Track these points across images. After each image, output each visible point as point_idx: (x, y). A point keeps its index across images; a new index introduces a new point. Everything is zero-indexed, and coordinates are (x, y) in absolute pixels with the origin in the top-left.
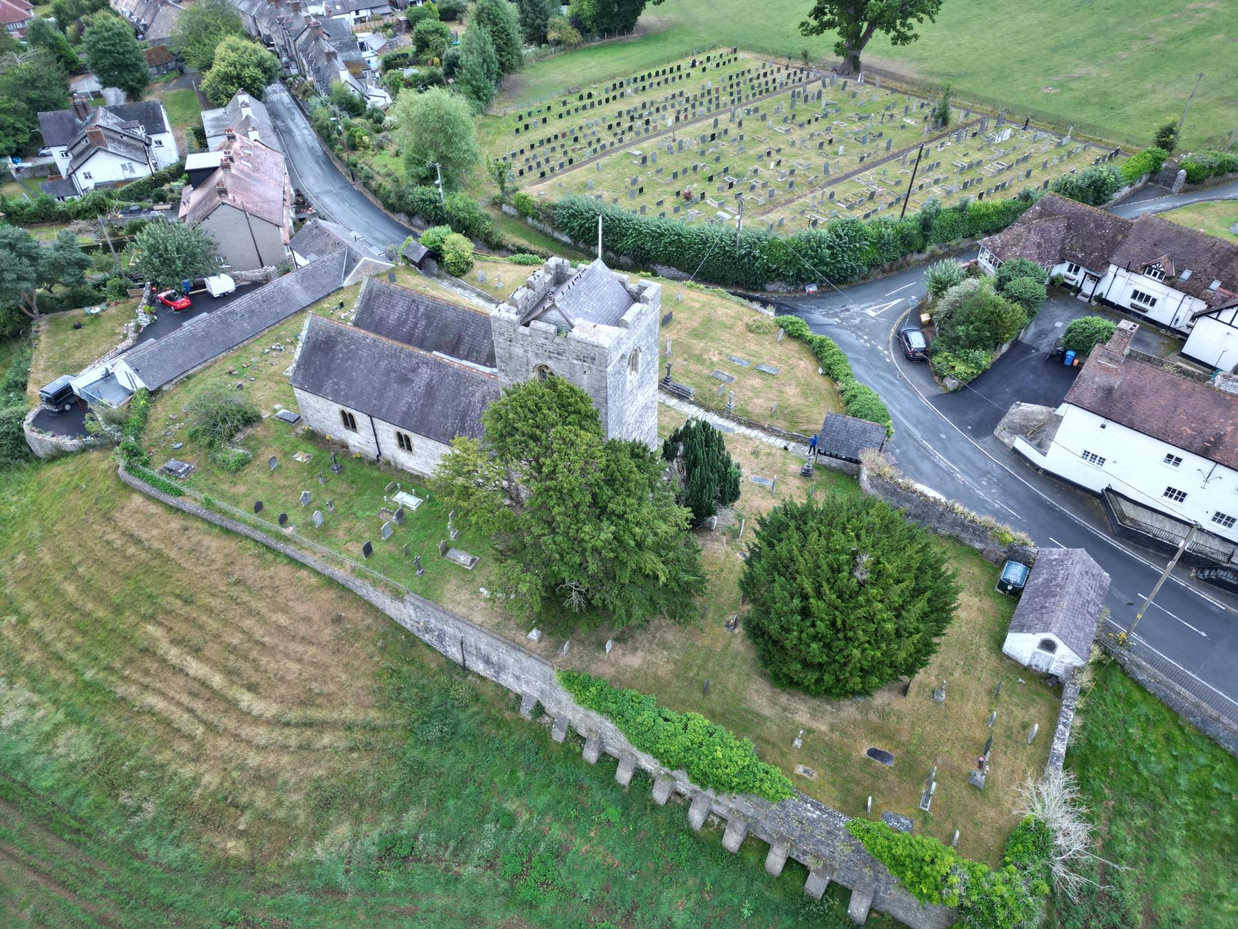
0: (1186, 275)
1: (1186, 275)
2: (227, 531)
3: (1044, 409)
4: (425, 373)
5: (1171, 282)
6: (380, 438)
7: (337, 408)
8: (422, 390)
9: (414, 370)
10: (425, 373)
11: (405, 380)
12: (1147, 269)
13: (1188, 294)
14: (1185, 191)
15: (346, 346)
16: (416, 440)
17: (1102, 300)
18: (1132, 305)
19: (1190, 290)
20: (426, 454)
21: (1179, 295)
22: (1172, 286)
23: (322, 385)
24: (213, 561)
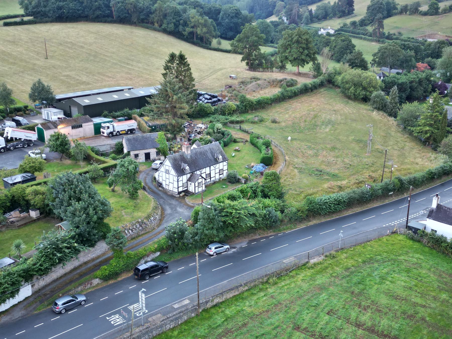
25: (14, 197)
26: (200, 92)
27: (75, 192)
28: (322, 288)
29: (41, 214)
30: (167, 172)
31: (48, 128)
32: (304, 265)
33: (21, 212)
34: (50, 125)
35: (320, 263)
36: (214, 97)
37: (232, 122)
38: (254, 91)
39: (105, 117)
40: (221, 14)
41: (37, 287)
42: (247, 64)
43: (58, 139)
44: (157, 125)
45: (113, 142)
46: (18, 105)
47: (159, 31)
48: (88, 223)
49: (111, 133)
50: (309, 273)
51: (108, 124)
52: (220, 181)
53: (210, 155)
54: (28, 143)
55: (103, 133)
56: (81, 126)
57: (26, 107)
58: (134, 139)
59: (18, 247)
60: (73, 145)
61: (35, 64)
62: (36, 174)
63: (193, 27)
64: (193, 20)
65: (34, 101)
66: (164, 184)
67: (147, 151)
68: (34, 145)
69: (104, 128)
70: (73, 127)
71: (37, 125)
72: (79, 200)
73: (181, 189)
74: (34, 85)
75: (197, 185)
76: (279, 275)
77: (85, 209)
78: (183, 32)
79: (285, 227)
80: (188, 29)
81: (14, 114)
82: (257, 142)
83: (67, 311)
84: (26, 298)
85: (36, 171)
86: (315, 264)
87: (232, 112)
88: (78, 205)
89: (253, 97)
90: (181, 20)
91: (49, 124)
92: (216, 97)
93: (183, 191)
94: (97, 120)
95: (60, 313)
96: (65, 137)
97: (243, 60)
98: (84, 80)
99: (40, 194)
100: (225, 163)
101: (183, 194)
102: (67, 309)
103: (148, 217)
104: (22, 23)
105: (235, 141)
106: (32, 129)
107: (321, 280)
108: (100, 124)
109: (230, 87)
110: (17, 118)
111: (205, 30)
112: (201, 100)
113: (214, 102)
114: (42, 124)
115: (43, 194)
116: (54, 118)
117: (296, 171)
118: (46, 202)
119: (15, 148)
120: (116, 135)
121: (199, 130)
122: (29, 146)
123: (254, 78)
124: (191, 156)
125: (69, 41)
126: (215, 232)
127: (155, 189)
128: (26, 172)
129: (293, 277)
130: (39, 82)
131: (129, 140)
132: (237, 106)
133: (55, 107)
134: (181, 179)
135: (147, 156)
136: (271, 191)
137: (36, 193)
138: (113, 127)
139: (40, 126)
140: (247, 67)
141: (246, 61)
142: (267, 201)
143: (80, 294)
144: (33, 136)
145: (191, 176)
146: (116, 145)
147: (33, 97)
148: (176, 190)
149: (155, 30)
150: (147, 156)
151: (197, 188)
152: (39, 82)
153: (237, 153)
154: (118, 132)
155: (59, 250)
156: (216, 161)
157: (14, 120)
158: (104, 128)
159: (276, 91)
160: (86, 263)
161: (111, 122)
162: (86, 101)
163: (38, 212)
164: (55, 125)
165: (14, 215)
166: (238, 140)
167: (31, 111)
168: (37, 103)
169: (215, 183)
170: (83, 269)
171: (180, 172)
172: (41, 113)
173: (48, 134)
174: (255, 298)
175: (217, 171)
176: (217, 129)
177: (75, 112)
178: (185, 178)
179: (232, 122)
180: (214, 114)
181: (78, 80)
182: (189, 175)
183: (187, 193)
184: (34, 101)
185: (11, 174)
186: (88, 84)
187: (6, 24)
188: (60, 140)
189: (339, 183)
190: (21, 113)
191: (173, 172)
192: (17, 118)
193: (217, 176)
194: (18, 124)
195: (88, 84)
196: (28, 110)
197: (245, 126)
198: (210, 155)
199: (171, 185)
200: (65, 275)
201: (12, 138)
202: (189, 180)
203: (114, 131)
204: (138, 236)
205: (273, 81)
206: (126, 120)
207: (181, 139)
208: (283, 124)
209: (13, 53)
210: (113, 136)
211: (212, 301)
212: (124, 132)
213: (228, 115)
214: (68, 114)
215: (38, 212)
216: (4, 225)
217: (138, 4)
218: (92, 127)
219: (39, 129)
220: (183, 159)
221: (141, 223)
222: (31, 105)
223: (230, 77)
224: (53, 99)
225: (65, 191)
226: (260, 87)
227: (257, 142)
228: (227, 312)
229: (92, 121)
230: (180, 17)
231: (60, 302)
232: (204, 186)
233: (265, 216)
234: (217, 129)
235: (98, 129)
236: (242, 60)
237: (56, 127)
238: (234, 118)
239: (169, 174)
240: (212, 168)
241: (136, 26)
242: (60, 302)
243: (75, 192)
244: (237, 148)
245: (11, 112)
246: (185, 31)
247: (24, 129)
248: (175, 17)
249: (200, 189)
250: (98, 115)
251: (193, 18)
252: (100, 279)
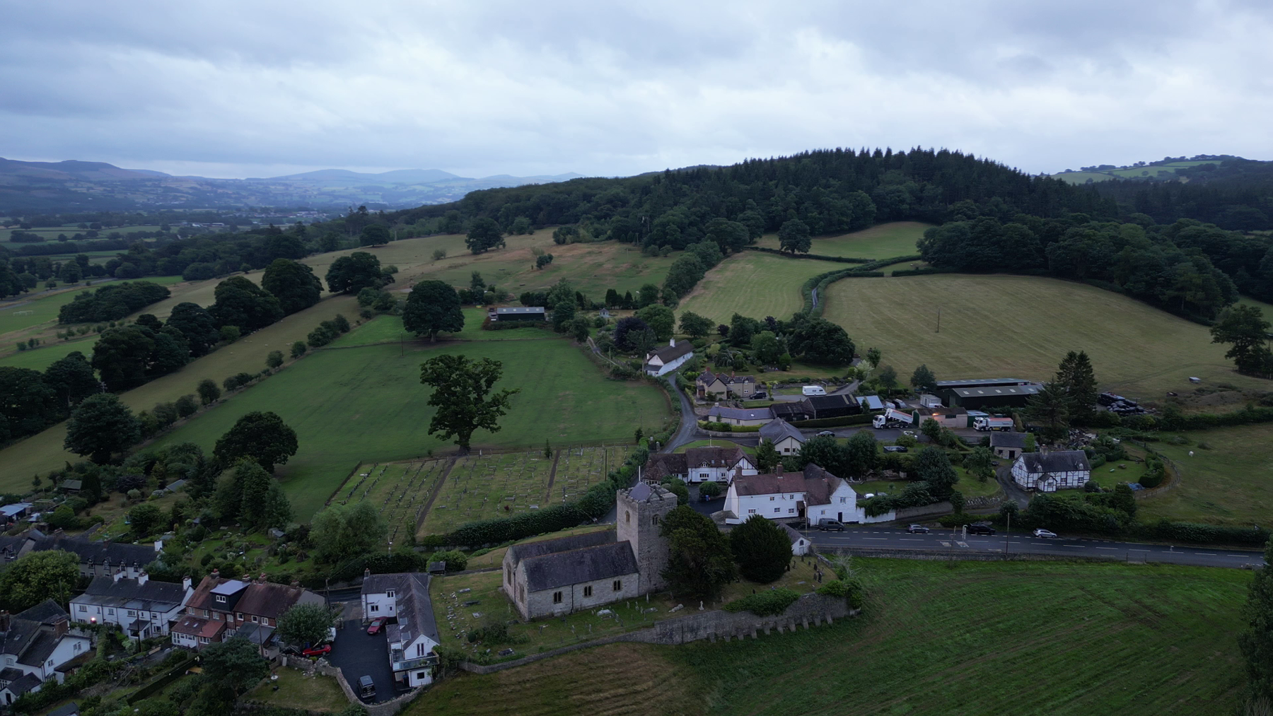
0: (713, 462)
1: (713, 462)
2: (560, 655)
3: (720, 512)
4: (587, 557)
5: (710, 466)
6: (574, 597)
7: (552, 593)
8: (590, 562)
9: (582, 557)
10: (587, 557)
11: (581, 563)
12: (700, 466)
13: (717, 467)
14: (662, 449)
15: (547, 564)
16: (596, 586)
17: (691, 482)
18: (702, 480)
19: (718, 466)
20: (598, 591)
21: (715, 469)
22: (712, 467)
23: (546, 585)
24: (568, 665)
25: (890, 459)
26: (1115, 397)
27: (934, 460)
28: (1123, 577)
29: (908, 476)
30: (1020, 468)
31: (924, 414)
32: (1121, 561)
33: (894, 472)
34: (926, 412)
35: (1138, 565)
36: (1132, 405)
37: (1140, 439)
38: (1210, 405)
39: (983, 411)
40: (1263, 259)
41: (899, 516)
42: (1237, 362)
43: (930, 424)
44: (1037, 427)
45: (981, 435)
46: (900, 388)
47: (1119, 292)
48: (940, 483)
49: (984, 427)
50: (1120, 567)
51: (982, 419)
52: (1078, 488)
53: (1070, 462)
54: (904, 424)
55: (976, 426)
56: (955, 417)
57: (906, 390)
58: (1001, 435)
59: (891, 487)
60: (942, 431)
61: (922, 339)
62: (908, 448)
63: (1178, 290)
64: (1182, 278)
65: (915, 385)
66: (1017, 477)
67: (1012, 449)
68: (909, 427)
69: (977, 421)
70: (947, 417)
71: (915, 409)
72: (936, 466)
73: (1030, 485)
74: (918, 369)
75: (1046, 484)
76: (1089, 561)
77: (939, 473)
78: (1160, 296)
79: (1127, 538)
80: (1171, 293)
81: (894, 397)
82: (1150, 463)
83: (916, 532)
84: (891, 521)
85: (909, 446)
86: (1131, 565)
87: (1147, 427)
88: (934, 469)
89: (1190, 413)
90: (1160, 277)
91: (926, 411)
92: (1135, 405)
93: (1032, 488)
94: (972, 413)
95: (911, 532)
96: (937, 423)
97: (1230, 355)
98: (976, 365)
99: (910, 460)
100: (1086, 472)
101: (1032, 490)
102: (916, 531)
103: (990, 497)
104: (917, 272)
105: (1127, 459)
106: (909, 412)
107: (1127, 573)
108: (974, 417)
109: (1175, 395)
110: (898, 400)
111: (1201, 295)
112: (1112, 406)
113: (1129, 412)
114: (919, 410)
115: (911, 461)
116: (931, 405)
117: (1179, 499)
118: (913, 466)
119: (892, 427)
120: (989, 430)
121: (1086, 440)
122: (904, 427)
123: (1224, 387)
124: (1047, 458)
125: (972, 306)
126: (1042, 517)
127: (1008, 482)
128: (901, 445)
129: (1103, 565)
130: (924, 367)
131: (995, 436)
132: (1159, 421)
133: (933, 394)
134: (1031, 475)
135: (1012, 454)
136: (1120, 502)
137: (907, 459)
138: (987, 422)
139: (917, 411)
140: (1237, 367)
141: (1234, 358)
142: (1111, 510)
143: (927, 527)
144: (909, 419)
145: (1043, 475)
146: (984, 438)
147: (914, 381)
148: (1026, 486)
149: (1113, 290)
150: (1012, 454)
151: (1046, 487)
152: (924, 367)
153: (1120, 470)
154: (991, 427)
155: (917, 494)
156: (1076, 469)
157: (894, 402)
158: (977, 421)
159: (1233, 409)
160: (934, 514)
161: (986, 416)
162: (966, 393)
163: (906, 473)
164: (931, 411)
165: (888, 473)
166: (1131, 458)
167: (910, 395)
168: (918, 388)
169: (1071, 488)
170: (930, 516)
171: (1032, 469)
172: (919, 398)
173: (922, 419)
174: (1058, 566)
175: (1076, 478)
176: (1107, 442)
177: (952, 401)
178: (1036, 476)
179: (1140, 439)
180: (1119, 425)
181: (968, 364)
182: (1040, 474)
183: (1036, 489)
184: (915, 385)
185: (890, 444)
186: (979, 370)
187: (896, 274)
188: (932, 425)
189: (1221, 518)
190: (901, 396)
191: (1025, 468)
192: (898, 400)
193: (1075, 484)
194: (898, 407)
195: (979, 370)
196: (907, 394)
197: (1151, 446)
198: (1070, 462)
199: (1022, 480)
200: (918, 516)
201: (891, 418)
202: (1040, 479)
203: (987, 426)
204: (979, 508)
205: (1255, 395)
206: (1004, 417)
207: (1059, 446)
208: (1214, 452)
209: (899, 322)
210: (985, 430)
211: (1020, 556)
212: (998, 429)
213: (1141, 429)
214: (945, 403)
215: (906, 473)
216: (881, 477)
217: (1091, 251)
218: (966, 418)
219: (915, 413)
220: (1039, 460)
221: (983, 499)
222: (911, 389)
223: (1191, 380)
224: (934, 385)
225: (927, 459)
226: (1223, 400)
227: (1150, 463)
228: (1030, 566)
229: (967, 413)
230: (1159, 272)
231: (913, 527)
232: (1055, 487)
233: (1102, 519)
234: (1107, 442)
235: (971, 421)
236: (1226, 356)
237: (931, 414)
238: (1149, 435)
239: (1021, 469)
240: (1069, 473)
241: (1082, 282)
242: (912, 526)
243: (934, 460)
244: (1122, 465)
245: (891, 394)
246: (1165, 294)
247: (902, 411)
248: (1150, 272)
249: (1050, 490)
250: (977, 409)
251: (1181, 276)
252: (941, 523)
